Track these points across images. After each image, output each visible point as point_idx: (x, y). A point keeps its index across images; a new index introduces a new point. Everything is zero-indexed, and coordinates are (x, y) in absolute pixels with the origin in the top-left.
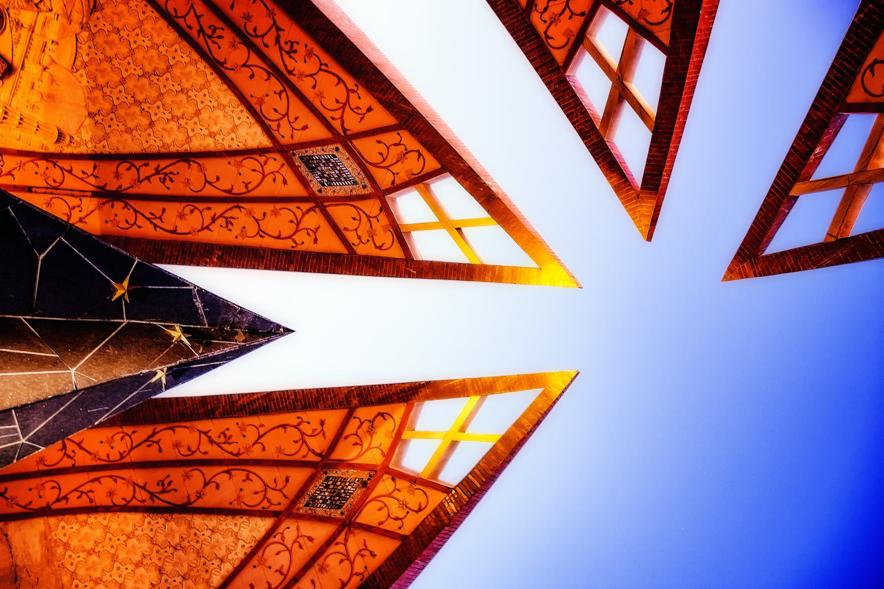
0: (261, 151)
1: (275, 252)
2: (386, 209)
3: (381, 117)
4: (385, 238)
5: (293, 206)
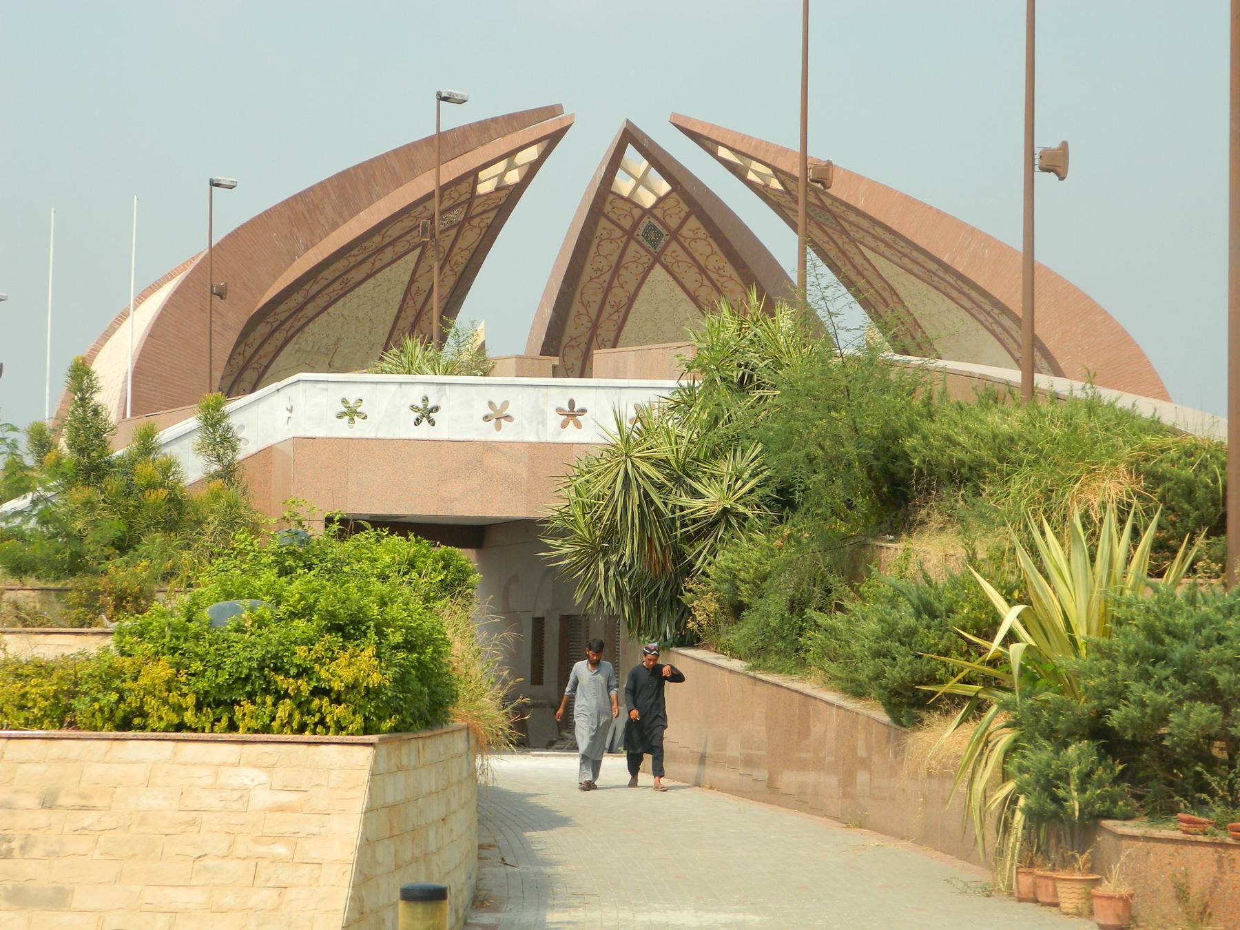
0: (665, 267)
1: (720, 245)
2: (654, 206)
3: (603, 222)
4: (671, 202)
5: (686, 244)
